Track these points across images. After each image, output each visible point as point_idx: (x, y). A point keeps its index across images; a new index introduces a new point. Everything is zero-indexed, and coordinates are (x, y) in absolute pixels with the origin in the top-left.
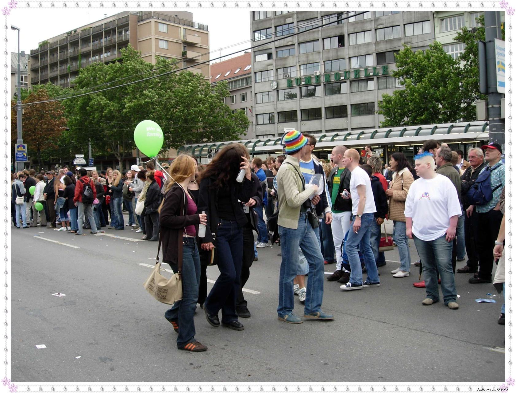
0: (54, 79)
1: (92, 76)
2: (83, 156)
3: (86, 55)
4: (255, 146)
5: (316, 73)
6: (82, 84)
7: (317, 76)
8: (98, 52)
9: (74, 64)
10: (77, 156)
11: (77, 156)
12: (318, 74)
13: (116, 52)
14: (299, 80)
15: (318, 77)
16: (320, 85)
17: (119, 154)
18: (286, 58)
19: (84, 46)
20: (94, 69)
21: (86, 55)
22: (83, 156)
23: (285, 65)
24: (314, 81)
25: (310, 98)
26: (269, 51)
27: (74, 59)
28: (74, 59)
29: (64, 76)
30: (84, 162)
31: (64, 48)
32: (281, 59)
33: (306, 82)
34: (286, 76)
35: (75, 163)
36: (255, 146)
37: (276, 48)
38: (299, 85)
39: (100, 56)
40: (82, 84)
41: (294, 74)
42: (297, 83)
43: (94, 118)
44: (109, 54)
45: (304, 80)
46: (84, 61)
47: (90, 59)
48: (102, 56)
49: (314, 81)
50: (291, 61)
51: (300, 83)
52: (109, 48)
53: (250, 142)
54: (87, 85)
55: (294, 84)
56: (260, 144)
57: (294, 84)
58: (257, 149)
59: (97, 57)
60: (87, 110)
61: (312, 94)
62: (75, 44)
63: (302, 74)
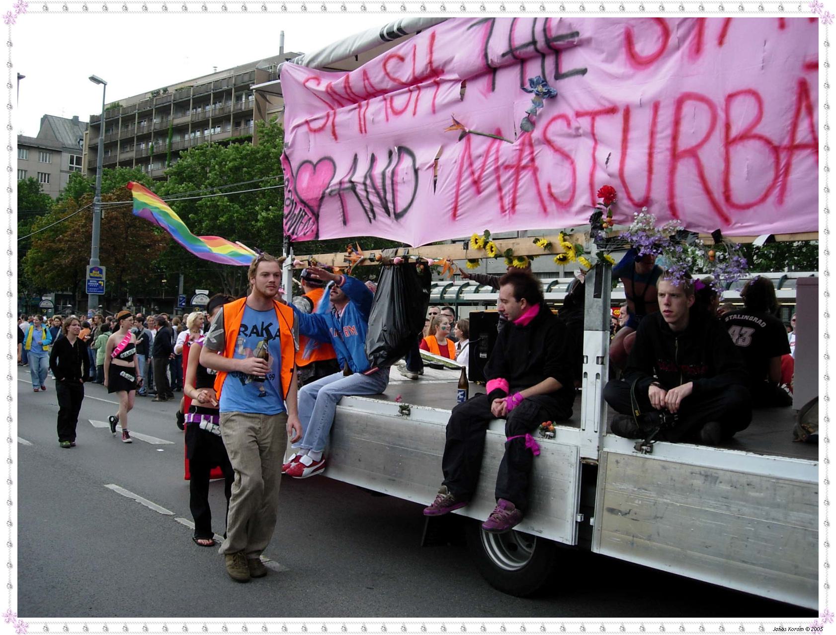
0: (127, 163)
1: (200, 164)
2: (207, 292)
3: (181, 130)
4: (460, 291)
6: (181, 176)
8: (201, 125)
9: (161, 142)
10: (197, 291)
11: (197, 291)
13: (229, 128)
17: (232, 291)
19: (180, 115)
20: (204, 154)
21: (181, 130)
22: (207, 292)
27: (161, 134)
28: (161, 134)
29: (145, 161)
30: (207, 300)
31: (146, 115)
35: (194, 303)
36: (460, 291)
39: (203, 133)
40: (181, 176)
44: (218, 130)
46: (177, 139)
47: (187, 136)
48: (206, 132)
52: (218, 121)
53: (451, 285)
54: (190, 178)
56: (468, 289)
58: (467, 296)
59: (198, 134)
62: (164, 111)
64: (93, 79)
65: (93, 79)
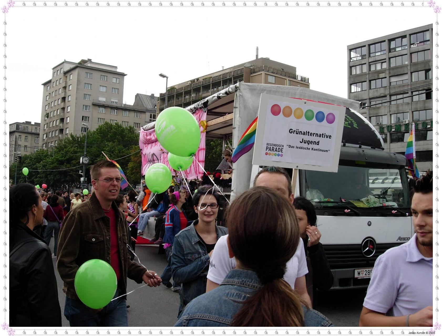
5: (405, 121)
7: (406, 124)
12: (407, 122)
14: (389, 127)
15: (407, 125)
16: (408, 132)
18: (379, 108)
19: (205, 92)
23: (377, 114)
24: (403, 129)
25: (399, 144)
26: (364, 102)
31: (188, 93)
32: (374, 108)
33: (396, 129)
34: (378, 123)
37: (370, 99)
38: (390, 132)
41: (385, 121)
42: (388, 130)
43: (216, 151)
45: (394, 127)
49: (403, 129)
50: (383, 110)
51: (391, 130)
55: (386, 131)
57: (386, 131)
60: (211, 144)
61: (401, 139)
62: (197, 90)
63: (392, 122)
64: (161, 75)
65: (161, 75)
